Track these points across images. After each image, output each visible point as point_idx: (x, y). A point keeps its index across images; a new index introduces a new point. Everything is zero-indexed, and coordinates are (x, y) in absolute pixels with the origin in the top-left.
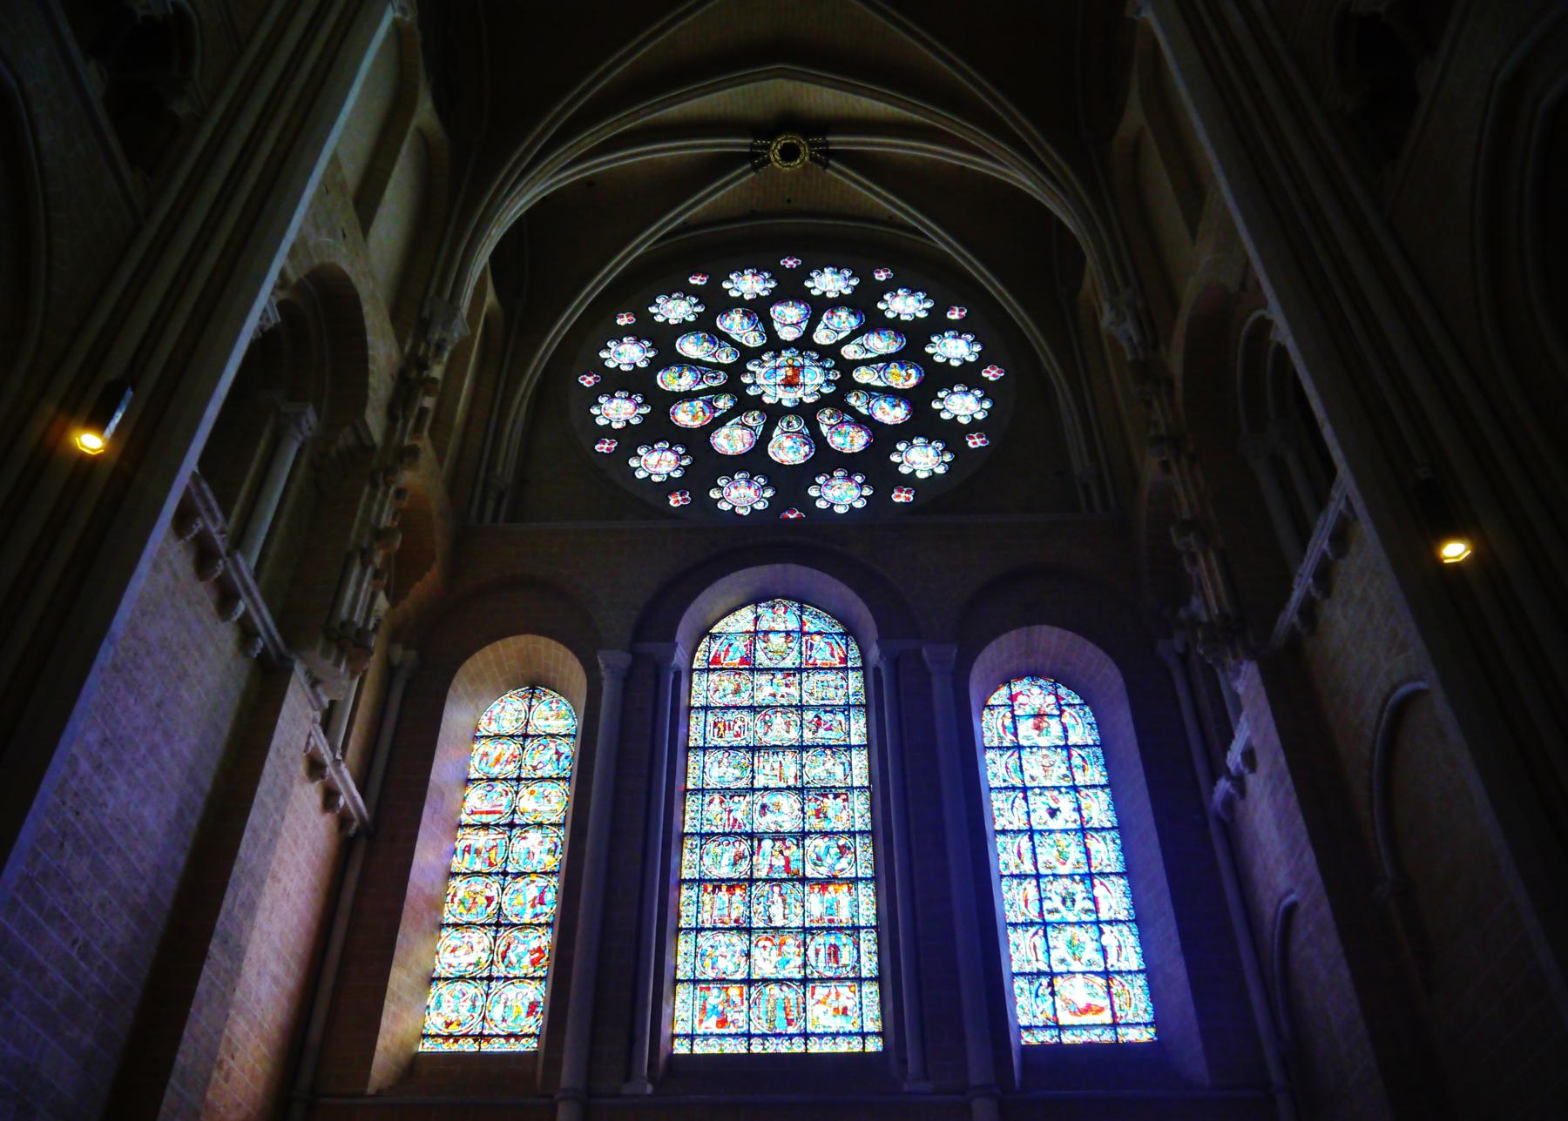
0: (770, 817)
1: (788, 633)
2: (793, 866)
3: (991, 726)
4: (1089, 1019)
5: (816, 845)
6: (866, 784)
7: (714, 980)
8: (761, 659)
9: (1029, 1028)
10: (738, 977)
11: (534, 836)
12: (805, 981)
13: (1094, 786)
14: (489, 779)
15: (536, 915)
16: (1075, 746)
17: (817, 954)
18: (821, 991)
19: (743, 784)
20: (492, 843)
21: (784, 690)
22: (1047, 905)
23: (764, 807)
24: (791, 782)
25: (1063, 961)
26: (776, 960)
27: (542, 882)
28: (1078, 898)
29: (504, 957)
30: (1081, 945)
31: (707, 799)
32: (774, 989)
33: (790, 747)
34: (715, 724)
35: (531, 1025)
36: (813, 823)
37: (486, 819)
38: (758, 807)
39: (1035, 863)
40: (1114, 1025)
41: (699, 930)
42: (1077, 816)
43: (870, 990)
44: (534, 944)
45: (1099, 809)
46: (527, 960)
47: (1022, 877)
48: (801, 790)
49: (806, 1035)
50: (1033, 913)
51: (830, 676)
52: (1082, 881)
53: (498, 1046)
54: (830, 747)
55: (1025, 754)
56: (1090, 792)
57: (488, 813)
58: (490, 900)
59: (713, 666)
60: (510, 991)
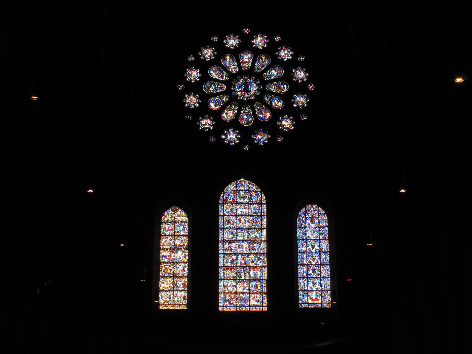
0: (240, 249)
1: (245, 191)
2: (246, 262)
3: (300, 219)
4: (316, 302)
5: (252, 257)
7: (228, 293)
8: (238, 200)
9: (301, 304)
10: (233, 292)
11: (180, 252)
12: (249, 293)
13: (324, 239)
14: (167, 236)
15: (183, 274)
16: (321, 227)
17: (252, 286)
18: (253, 296)
19: (234, 239)
20: (169, 254)
21: (244, 210)
22: (309, 273)
24: (246, 239)
25: (311, 287)
26: (242, 290)
27: (183, 265)
28: (317, 271)
29: (176, 285)
30: (316, 283)
31: (225, 243)
32: (241, 295)
35: (185, 302)
36: (252, 251)
37: (167, 247)
38: (237, 246)
39: (307, 261)
40: (322, 303)
41: (224, 279)
42: (318, 248)
43: (265, 296)
44: (183, 282)
45: (325, 246)
46: (181, 286)
47: (304, 265)
48: (249, 241)
49: (249, 306)
50: (305, 274)
51: (257, 206)
52: (318, 266)
53: (177, 307)
54: (256, 228)
55: (308, 229)
56: (323, 241)
57: (167, 245)
58: (171, 270)
59: (225, 202)
60: (179, 294)
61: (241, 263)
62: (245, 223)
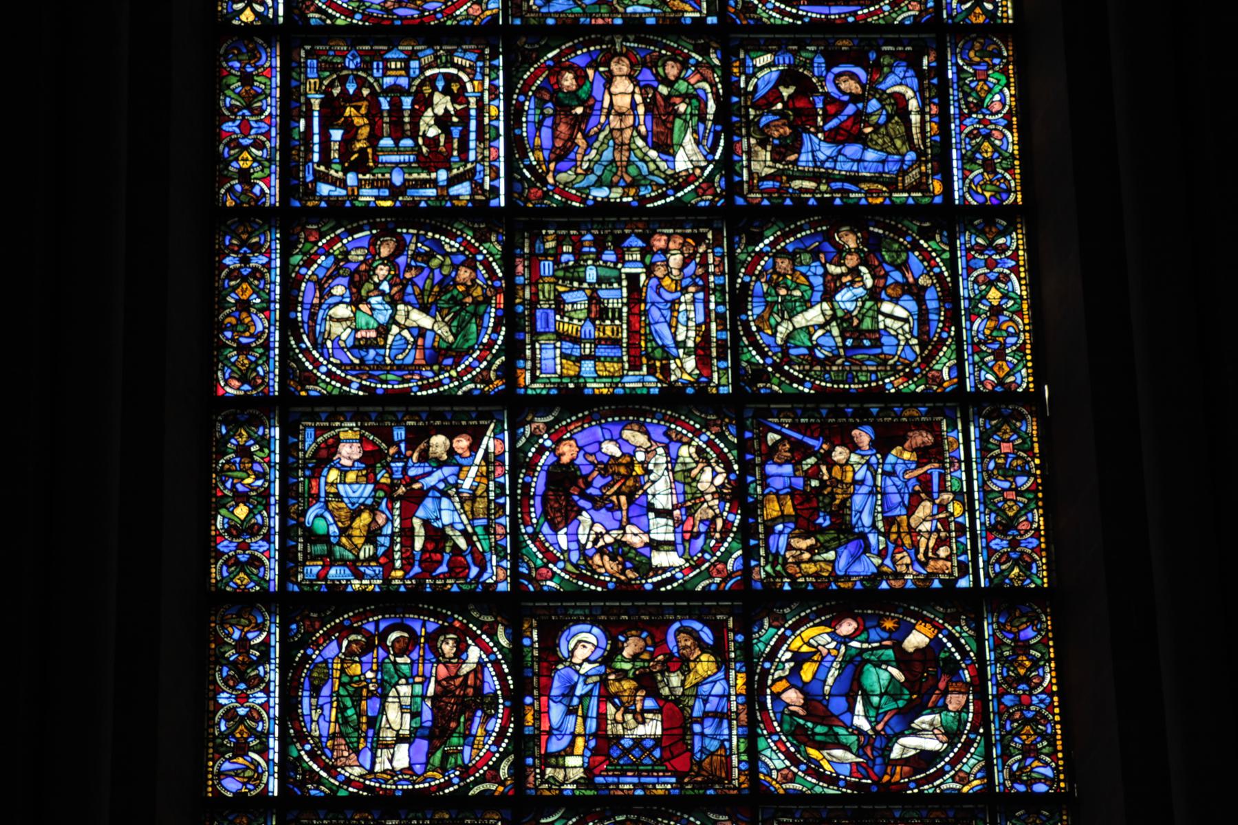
0: (588, 526)
6: (1023, 379)
19: (457, 380)
23: (564, 479)
31: (309, 442)
33: (677, 216)
34: (332, 112)
54: (856, 216)
61: (603, 743)
62: (666, 147)
